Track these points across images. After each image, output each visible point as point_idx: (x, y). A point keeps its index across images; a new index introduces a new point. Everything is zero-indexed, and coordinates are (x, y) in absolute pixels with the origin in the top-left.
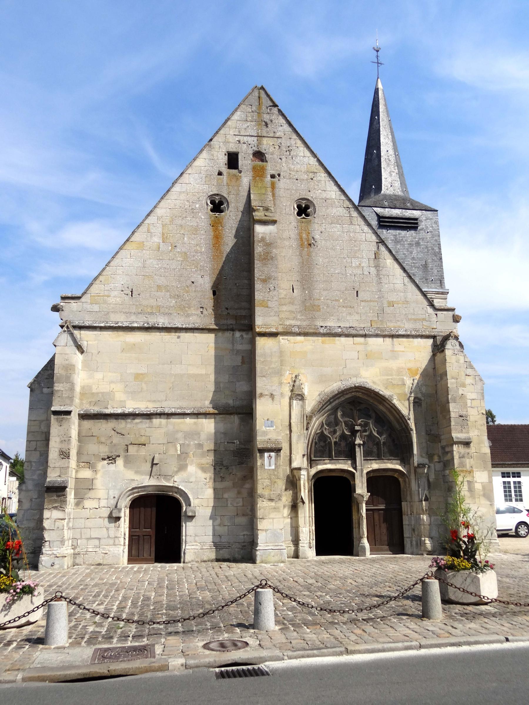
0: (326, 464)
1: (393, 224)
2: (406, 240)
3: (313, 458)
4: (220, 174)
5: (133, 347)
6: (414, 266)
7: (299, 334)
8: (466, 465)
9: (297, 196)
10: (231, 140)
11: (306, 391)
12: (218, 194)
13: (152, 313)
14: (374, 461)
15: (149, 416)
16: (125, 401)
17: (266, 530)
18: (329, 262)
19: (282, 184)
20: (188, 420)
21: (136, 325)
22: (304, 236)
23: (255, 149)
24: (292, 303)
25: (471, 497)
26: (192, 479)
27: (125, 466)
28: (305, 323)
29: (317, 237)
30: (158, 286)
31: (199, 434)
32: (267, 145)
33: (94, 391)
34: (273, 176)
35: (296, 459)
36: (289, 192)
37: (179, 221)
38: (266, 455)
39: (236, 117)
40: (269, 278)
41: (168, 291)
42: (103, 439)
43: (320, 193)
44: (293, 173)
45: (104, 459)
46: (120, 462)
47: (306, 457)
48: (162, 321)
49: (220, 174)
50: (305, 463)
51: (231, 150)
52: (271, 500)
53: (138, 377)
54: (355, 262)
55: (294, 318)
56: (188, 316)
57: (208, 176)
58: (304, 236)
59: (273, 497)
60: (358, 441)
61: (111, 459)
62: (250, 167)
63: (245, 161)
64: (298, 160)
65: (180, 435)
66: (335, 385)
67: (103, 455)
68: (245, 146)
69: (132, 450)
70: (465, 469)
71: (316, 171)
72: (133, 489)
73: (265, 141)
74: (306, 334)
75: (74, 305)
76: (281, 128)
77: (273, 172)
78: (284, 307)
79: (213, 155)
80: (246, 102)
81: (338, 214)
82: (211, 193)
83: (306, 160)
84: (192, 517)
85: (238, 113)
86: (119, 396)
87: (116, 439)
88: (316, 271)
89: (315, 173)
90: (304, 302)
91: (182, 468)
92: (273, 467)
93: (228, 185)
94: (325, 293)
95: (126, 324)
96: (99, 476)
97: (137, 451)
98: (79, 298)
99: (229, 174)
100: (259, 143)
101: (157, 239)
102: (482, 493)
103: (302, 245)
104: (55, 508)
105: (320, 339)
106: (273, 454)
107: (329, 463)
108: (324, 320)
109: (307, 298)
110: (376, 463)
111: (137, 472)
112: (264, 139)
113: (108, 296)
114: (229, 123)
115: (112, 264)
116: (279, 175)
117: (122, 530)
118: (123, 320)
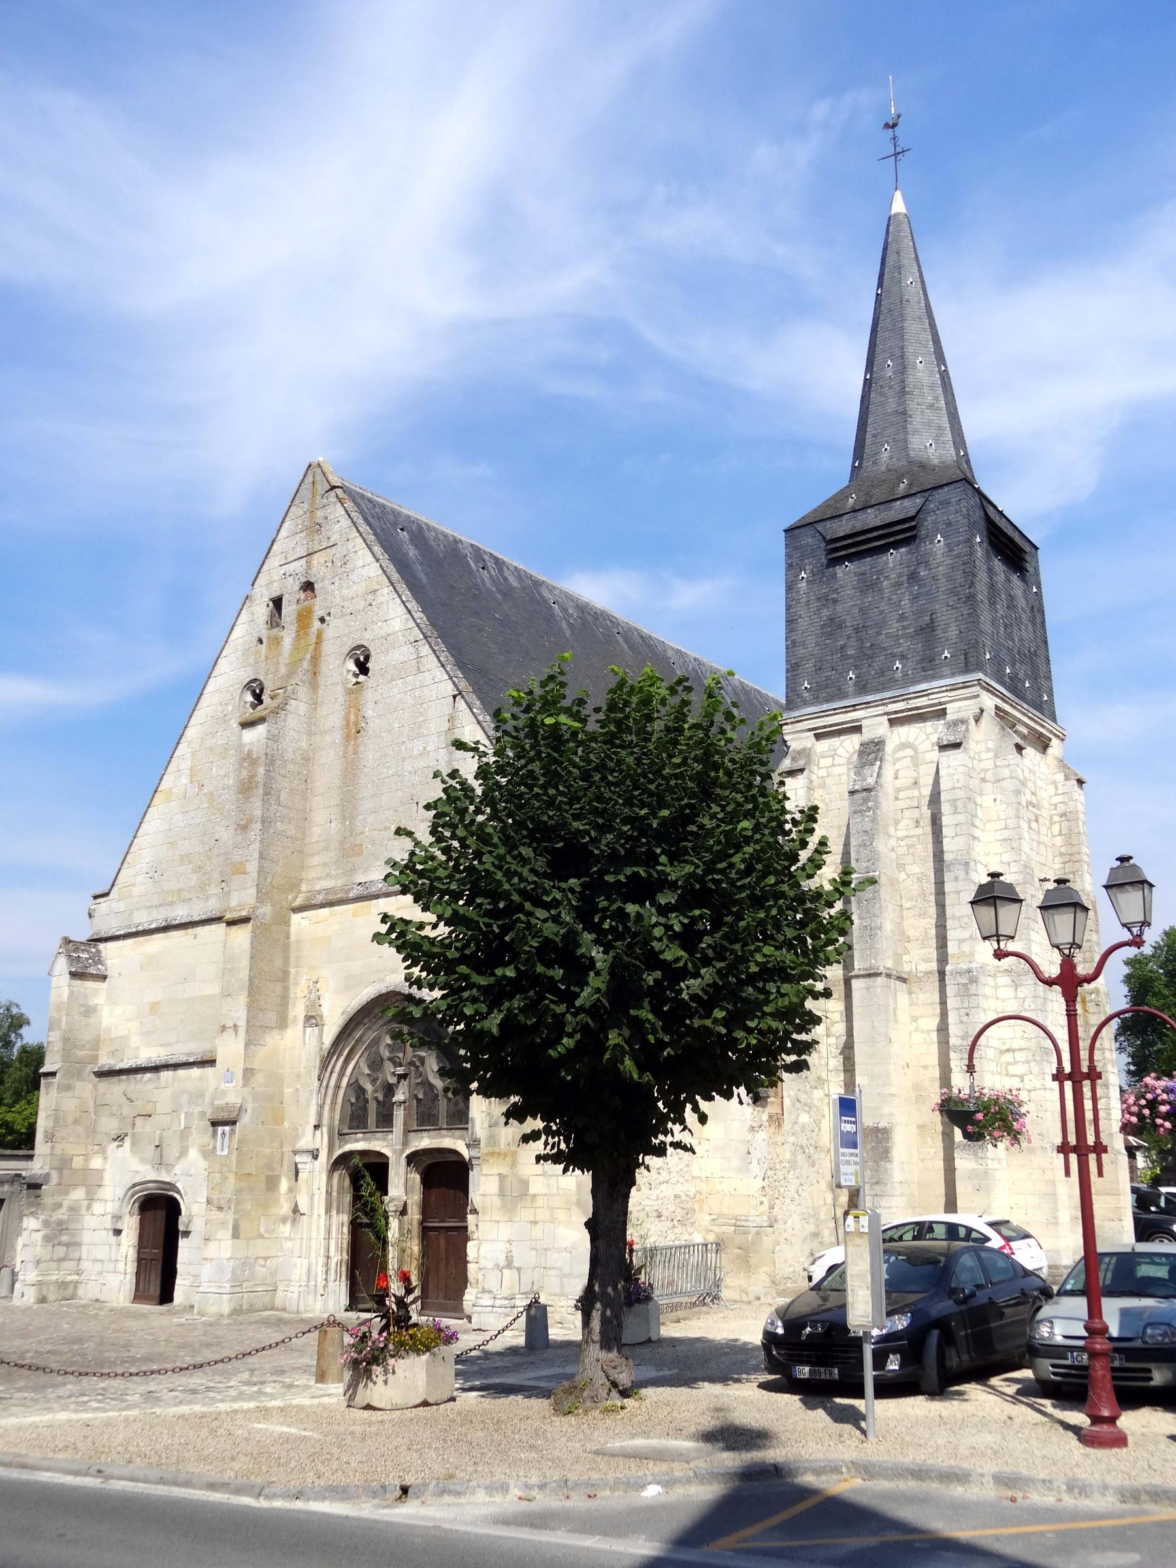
0: (357, 1141)
1: (864, 547)
2: (887, 578)
3: (346, 1131)
4: (261, 641)
5: (150, 962)
6: (902, 637)
7: (322, 906)
8: (499, 1140)
9: (350, 645)
10: (275, 578)
11: (325, 1010)
12: (256, 679)
13: (172, 903)
14: (425, 1134)
15: (156, 1069)
16: (138, 1048)
17: (212, 1259)
18: (381, 757)
19: (330, 632)
20: (195, 1072)
21: (153, 926)
22: (352, 717)
23: (303, 580)
24: (326, 849)
25: (502, 1207)
26: (192, 1172)
27: (131, 1151)
28: (339, 883)
29: (369, 713)
30: (182, 856)
31: (202, 1095)
32: (319, 568)
33: (113, 1036)
34: (322, 620)
35: (304, 1134)
36: (339, 642)
37: (209, 743)
38: (220, 1129)
39: (283, 533)
40: (251, 821)
41: (190, 862)
42: (114, 1109)
43: (380, 627)
44: (346, 604)
45: (115, 1140)
46: (127, 1142)
47: (325, 1130)
48: (181, 913)
49: (261, 641)
50: (320, 1141)
51: (275, 595)
52: (220, 1208)
53: (154, 1007)
54: (418, 746)
55: (328, 876)
56: (207, 898)
57: (246, 652)
58: (352, 717)
59: (223, 1203)
60: (399, 1096)
61: (120, 1138)
62: (294, 617)
63: (288, 609)
64: (353, 577)
65: (184, 1098)
66: (365, 992)
67: (114, 1134)
68: (291, 579)
69: (139, 1121)
70: (497, 1150)
71: (376, 587)
72: (134, 1186)
73: (317, 559)
74: (331, 904)
75: (103, 905)
76: (336, 527)
77: (321, 613)
78: (317, 857)
79: (253, 614)
80: (297, 502)
81: (402, 659)
82: (248, 680)
83: (364, 572)
84: (187, 1234)
85: (286, 525)
86: (135, 1041)
87: (126, 1110)
88: (363, 780)
89: (374, 592)
90: (342, 843)
91: (183, 1152)
92: (226, 1152)
93: (267, 658)
94: (370, 819)
95: (146, 927)
96: (108, 1166)
97: (143, 1127)
98: (107, 894)
99: (269, 637)
100: (309, 565)
101: (184, 780)
102: (574, 1199)
103: (347, 737)
104: (32, 1213)
105: (350, 907)
106: (227, 1129)
107: (363, 1139)
108: (366, 870)
109: (348, 833)
110: (429, 1137)
111: (143, 1160)
112: (315, 556)
113: (134, 885)
114: (275, 547)
115: (139, 834)
116: (329, 614)
117: (123, 1249)
118: (143, 919)
